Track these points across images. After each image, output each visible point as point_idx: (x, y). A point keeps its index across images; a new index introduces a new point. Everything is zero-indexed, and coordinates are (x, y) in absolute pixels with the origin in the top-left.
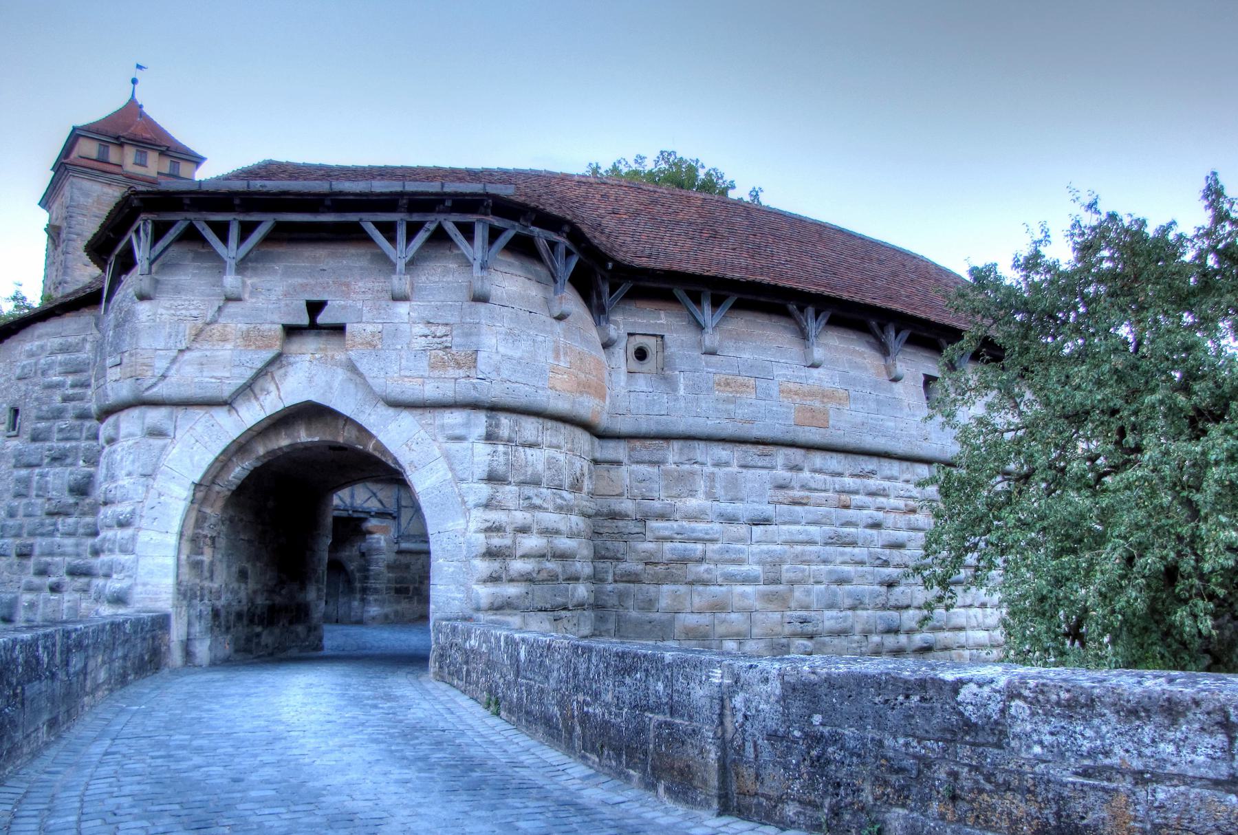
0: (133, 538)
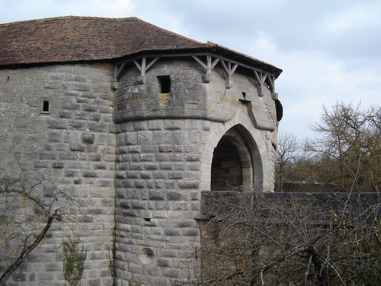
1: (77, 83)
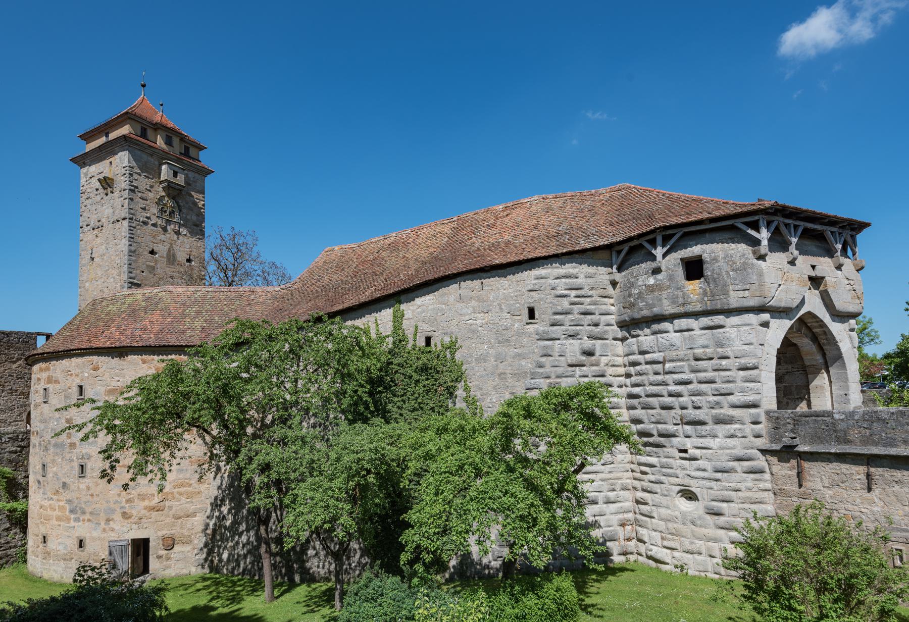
0: (759, 375)
1: (567, 280)
